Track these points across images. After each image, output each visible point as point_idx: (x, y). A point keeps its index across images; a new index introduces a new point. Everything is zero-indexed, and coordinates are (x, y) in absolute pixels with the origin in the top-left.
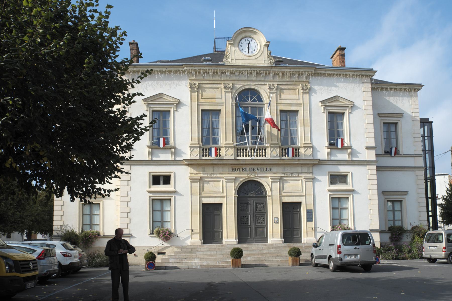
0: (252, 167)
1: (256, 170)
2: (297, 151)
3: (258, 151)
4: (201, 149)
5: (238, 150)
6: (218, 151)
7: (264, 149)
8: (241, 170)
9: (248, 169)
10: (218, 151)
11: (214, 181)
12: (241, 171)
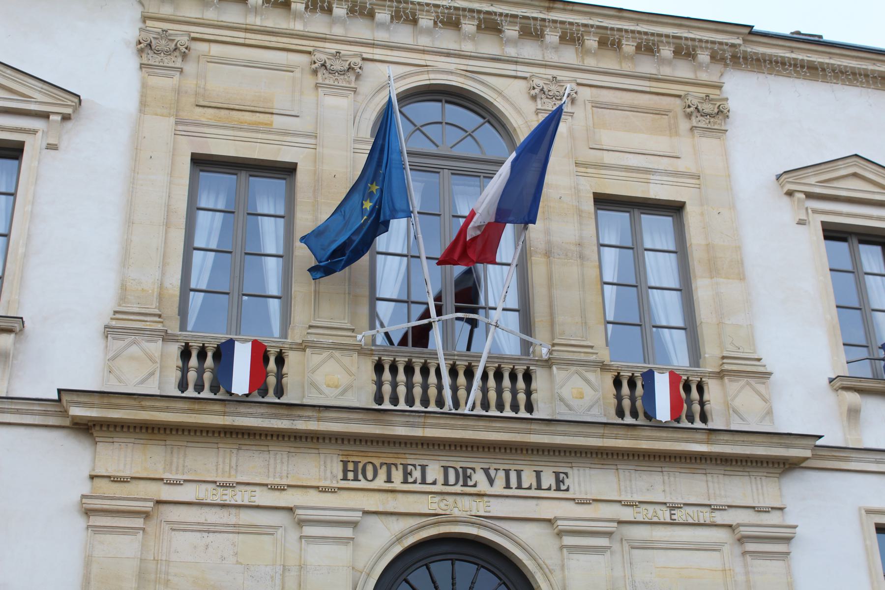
0: (459, 462)
1: (479, 477)
2: (695, 394)
3: (491, 382)
4: (174, 350)
5: (379, 368)
6: (272, 365)
7: (520, 369)
8: (397, 475)
9: (434, 472)
10: (272, 365)
11: (237, 529)
12: (397, 484)
